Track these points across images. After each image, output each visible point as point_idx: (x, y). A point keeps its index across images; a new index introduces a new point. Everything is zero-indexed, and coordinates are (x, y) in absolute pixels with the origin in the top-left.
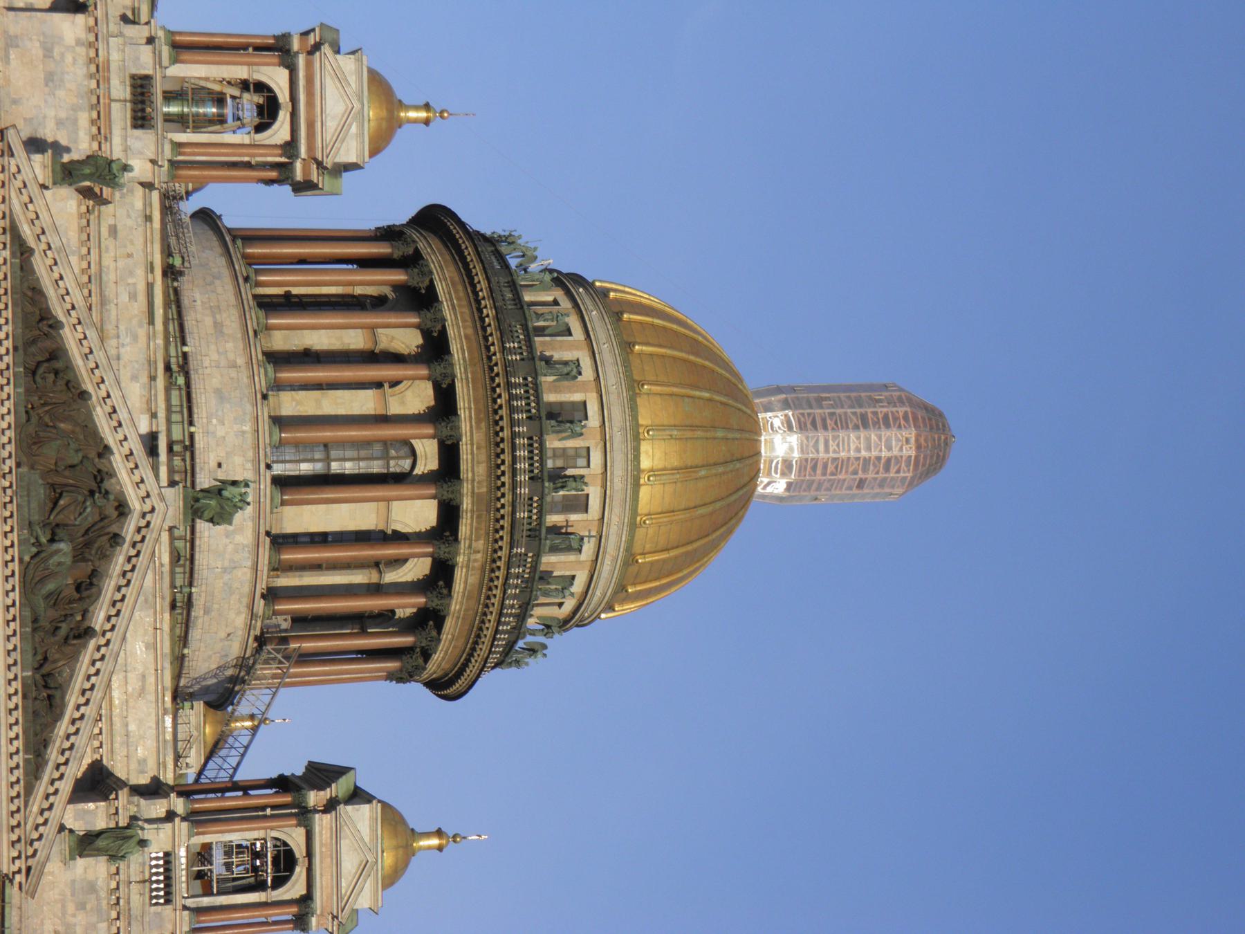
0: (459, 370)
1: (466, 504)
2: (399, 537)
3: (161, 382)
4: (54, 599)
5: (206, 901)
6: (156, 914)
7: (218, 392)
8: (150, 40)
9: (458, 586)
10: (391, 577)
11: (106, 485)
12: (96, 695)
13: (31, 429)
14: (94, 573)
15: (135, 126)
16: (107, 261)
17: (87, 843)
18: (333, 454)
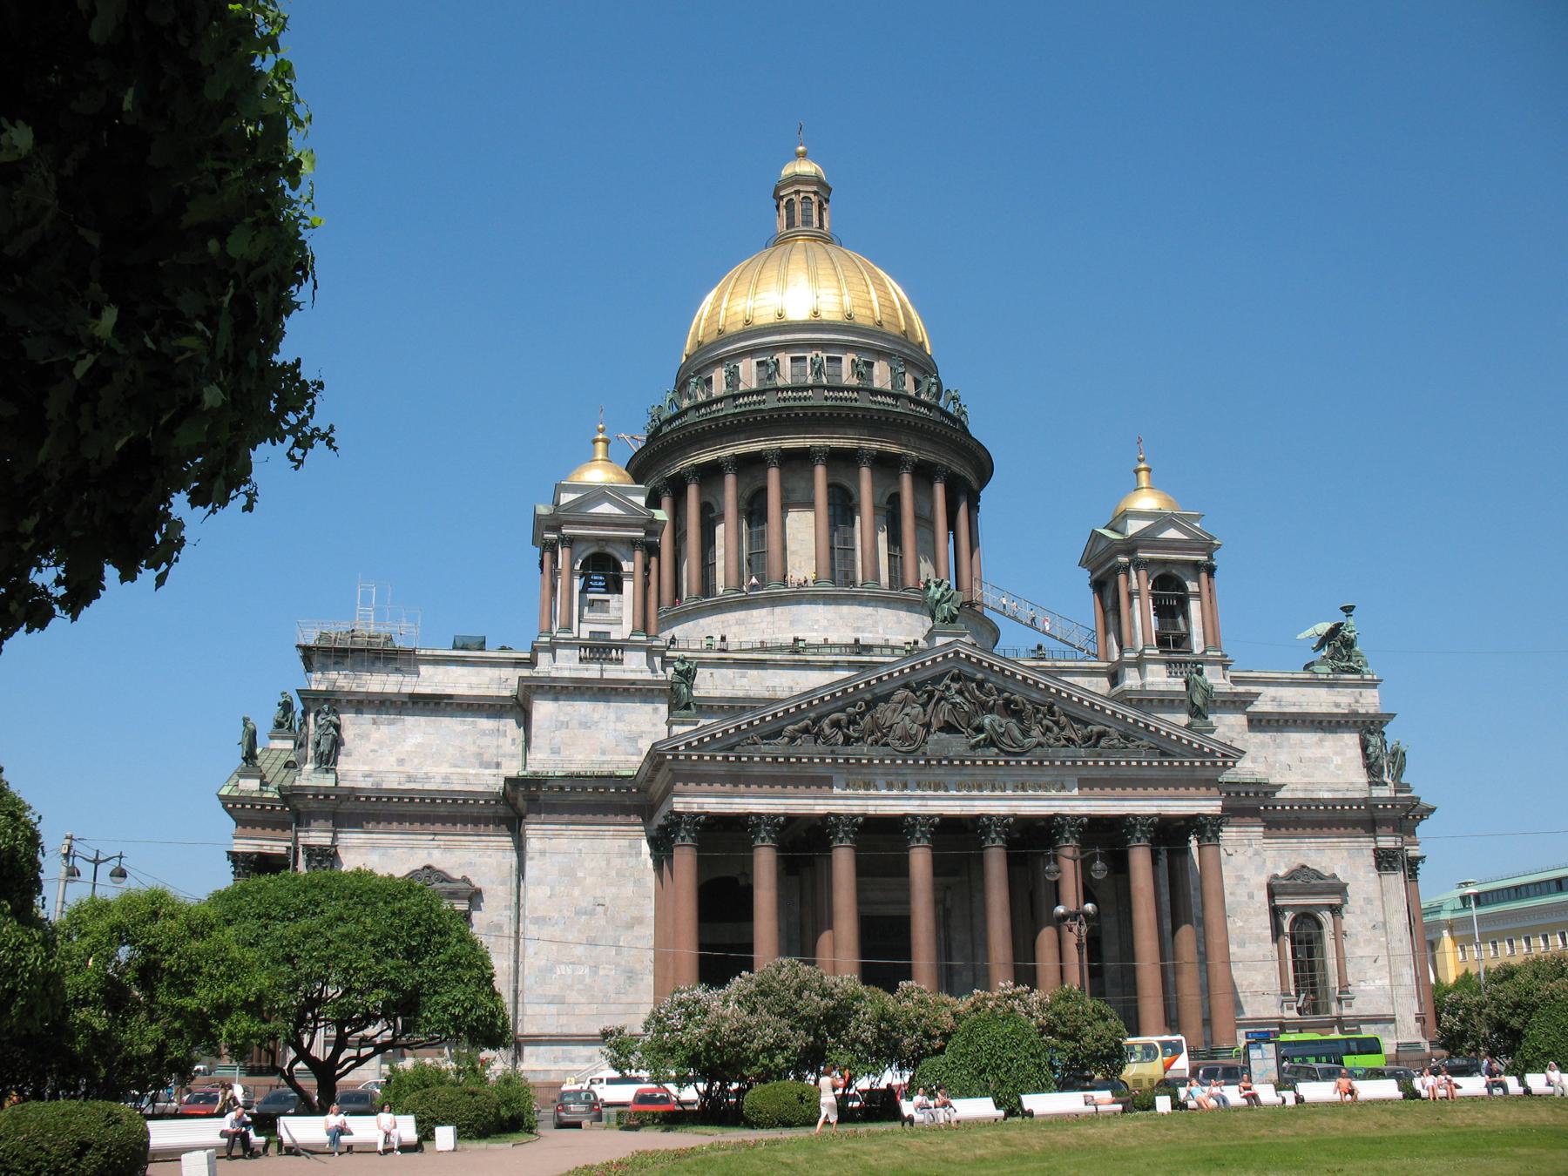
0: (775, 445)
1: (876, 446)
6: (1210, 674)
7: (792, 623)
9: (932, 457)
12: (1098, 701)
15: (620, 661)
16: (717, 694)
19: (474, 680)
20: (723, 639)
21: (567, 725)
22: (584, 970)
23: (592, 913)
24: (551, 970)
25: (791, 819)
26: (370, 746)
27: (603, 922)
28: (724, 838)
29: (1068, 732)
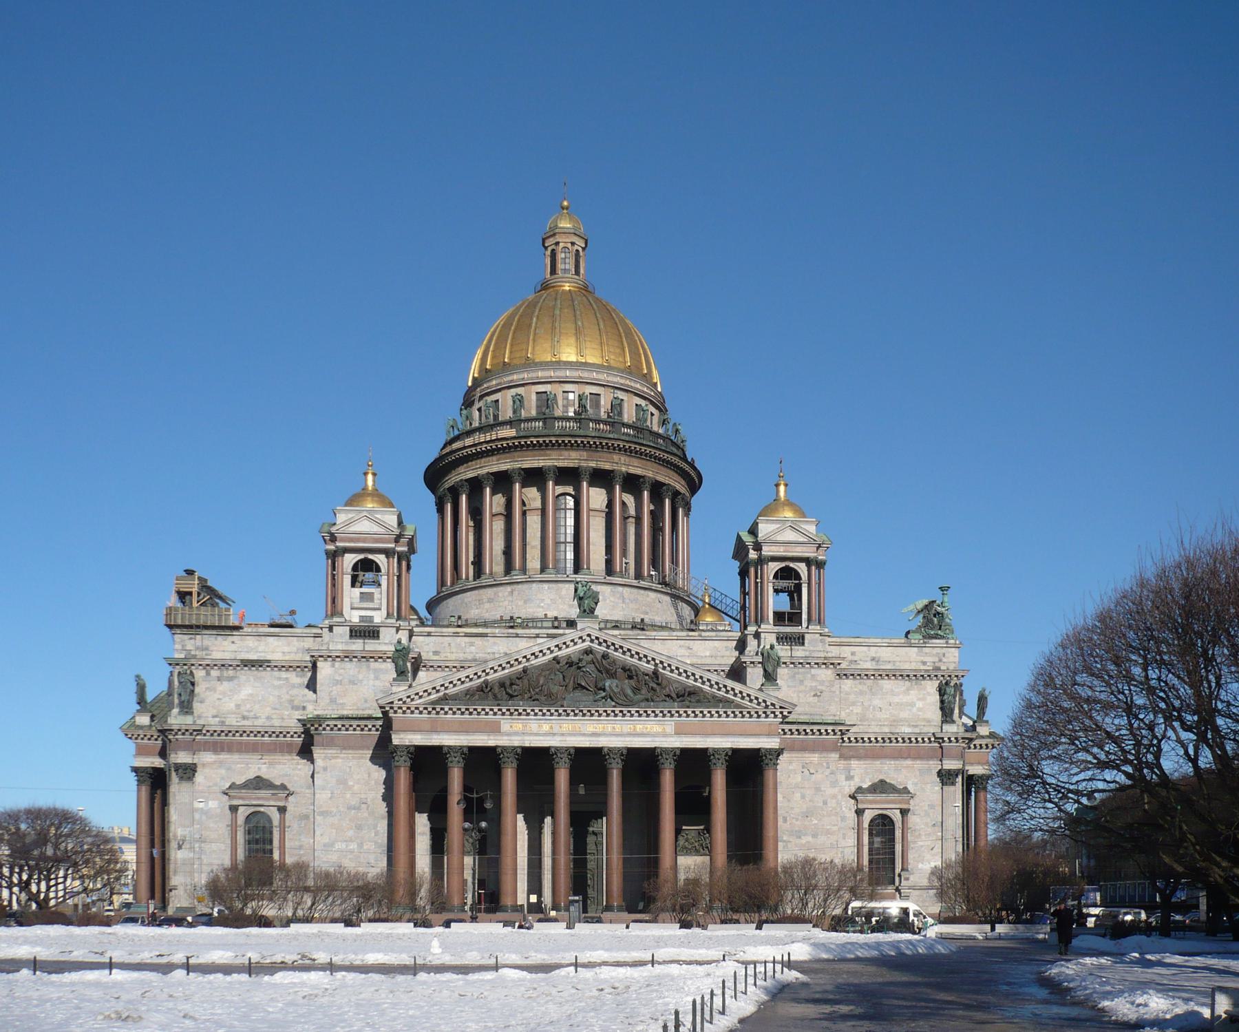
0: (517, 465)
1: (593, 464)
2: (610, 505)
3: (519, 631)
4: (636, 690)
5: (805, 616)
7: (525, 602)
8: (331, 629)
9: (639, 472)
10: (632, 511)
11: (575, 660)
12: (690, 670)
13: (543, 698)
14: (624, 669)
17: (770, 677)
18: (562, 540)
19: (286, 649)
20: (459, 618)
21: (339, 682)
22: (353, 846)
23: (358, 809)
24: (332, 845)
25: (472, 749)
26: (217, 696)
27: (366, 815)
28: (428, 762)
29: (666, 691)
